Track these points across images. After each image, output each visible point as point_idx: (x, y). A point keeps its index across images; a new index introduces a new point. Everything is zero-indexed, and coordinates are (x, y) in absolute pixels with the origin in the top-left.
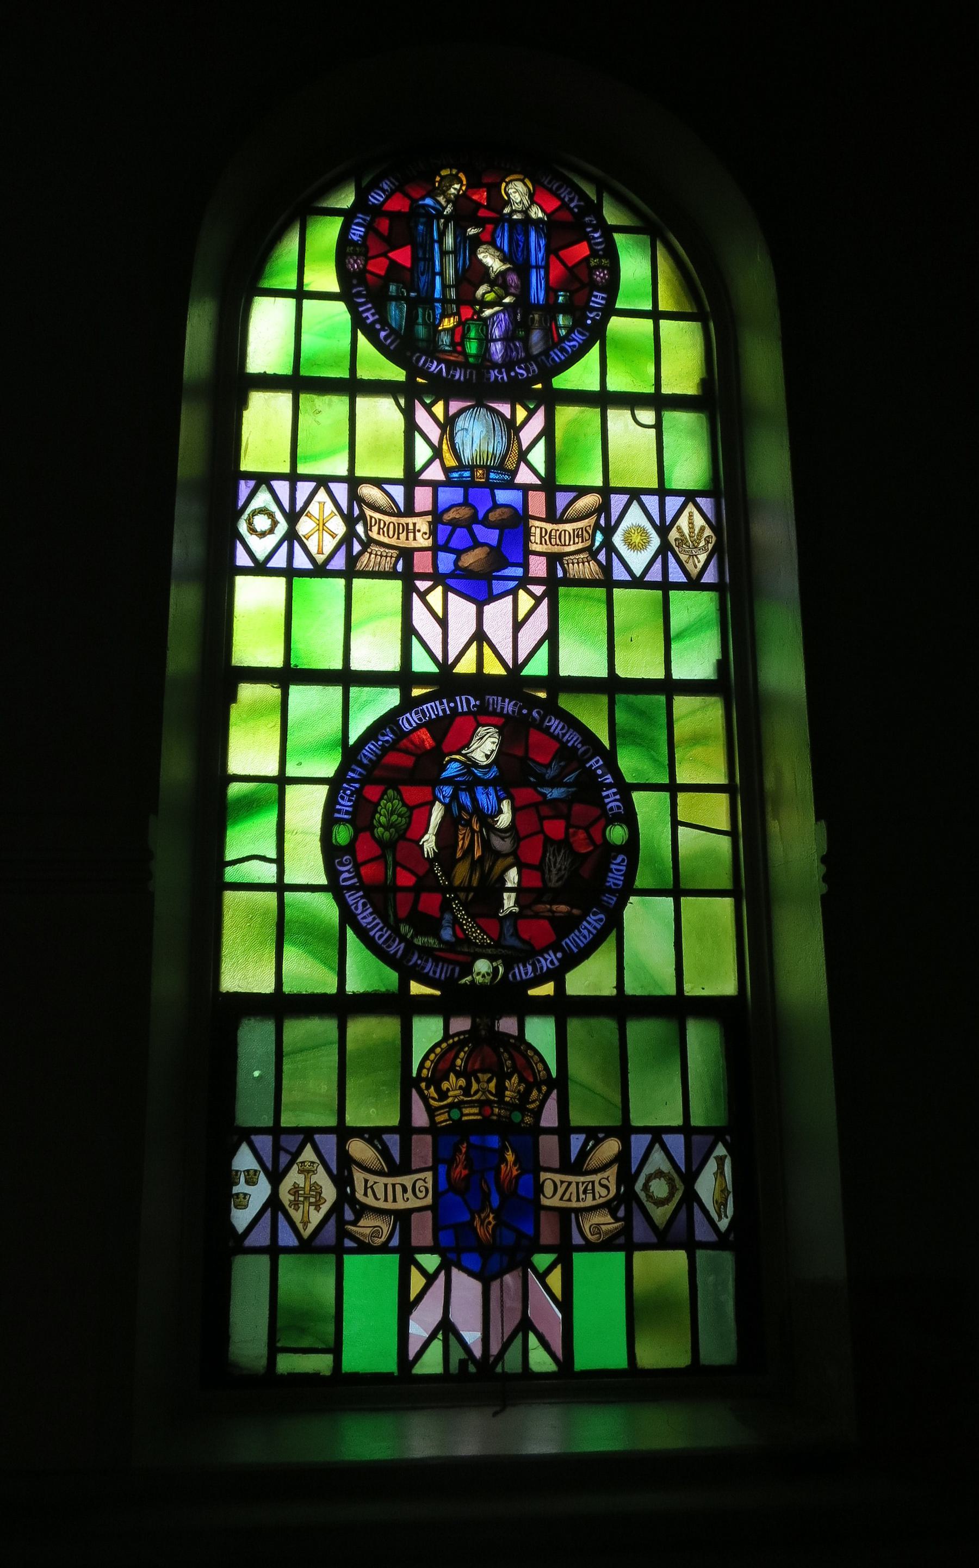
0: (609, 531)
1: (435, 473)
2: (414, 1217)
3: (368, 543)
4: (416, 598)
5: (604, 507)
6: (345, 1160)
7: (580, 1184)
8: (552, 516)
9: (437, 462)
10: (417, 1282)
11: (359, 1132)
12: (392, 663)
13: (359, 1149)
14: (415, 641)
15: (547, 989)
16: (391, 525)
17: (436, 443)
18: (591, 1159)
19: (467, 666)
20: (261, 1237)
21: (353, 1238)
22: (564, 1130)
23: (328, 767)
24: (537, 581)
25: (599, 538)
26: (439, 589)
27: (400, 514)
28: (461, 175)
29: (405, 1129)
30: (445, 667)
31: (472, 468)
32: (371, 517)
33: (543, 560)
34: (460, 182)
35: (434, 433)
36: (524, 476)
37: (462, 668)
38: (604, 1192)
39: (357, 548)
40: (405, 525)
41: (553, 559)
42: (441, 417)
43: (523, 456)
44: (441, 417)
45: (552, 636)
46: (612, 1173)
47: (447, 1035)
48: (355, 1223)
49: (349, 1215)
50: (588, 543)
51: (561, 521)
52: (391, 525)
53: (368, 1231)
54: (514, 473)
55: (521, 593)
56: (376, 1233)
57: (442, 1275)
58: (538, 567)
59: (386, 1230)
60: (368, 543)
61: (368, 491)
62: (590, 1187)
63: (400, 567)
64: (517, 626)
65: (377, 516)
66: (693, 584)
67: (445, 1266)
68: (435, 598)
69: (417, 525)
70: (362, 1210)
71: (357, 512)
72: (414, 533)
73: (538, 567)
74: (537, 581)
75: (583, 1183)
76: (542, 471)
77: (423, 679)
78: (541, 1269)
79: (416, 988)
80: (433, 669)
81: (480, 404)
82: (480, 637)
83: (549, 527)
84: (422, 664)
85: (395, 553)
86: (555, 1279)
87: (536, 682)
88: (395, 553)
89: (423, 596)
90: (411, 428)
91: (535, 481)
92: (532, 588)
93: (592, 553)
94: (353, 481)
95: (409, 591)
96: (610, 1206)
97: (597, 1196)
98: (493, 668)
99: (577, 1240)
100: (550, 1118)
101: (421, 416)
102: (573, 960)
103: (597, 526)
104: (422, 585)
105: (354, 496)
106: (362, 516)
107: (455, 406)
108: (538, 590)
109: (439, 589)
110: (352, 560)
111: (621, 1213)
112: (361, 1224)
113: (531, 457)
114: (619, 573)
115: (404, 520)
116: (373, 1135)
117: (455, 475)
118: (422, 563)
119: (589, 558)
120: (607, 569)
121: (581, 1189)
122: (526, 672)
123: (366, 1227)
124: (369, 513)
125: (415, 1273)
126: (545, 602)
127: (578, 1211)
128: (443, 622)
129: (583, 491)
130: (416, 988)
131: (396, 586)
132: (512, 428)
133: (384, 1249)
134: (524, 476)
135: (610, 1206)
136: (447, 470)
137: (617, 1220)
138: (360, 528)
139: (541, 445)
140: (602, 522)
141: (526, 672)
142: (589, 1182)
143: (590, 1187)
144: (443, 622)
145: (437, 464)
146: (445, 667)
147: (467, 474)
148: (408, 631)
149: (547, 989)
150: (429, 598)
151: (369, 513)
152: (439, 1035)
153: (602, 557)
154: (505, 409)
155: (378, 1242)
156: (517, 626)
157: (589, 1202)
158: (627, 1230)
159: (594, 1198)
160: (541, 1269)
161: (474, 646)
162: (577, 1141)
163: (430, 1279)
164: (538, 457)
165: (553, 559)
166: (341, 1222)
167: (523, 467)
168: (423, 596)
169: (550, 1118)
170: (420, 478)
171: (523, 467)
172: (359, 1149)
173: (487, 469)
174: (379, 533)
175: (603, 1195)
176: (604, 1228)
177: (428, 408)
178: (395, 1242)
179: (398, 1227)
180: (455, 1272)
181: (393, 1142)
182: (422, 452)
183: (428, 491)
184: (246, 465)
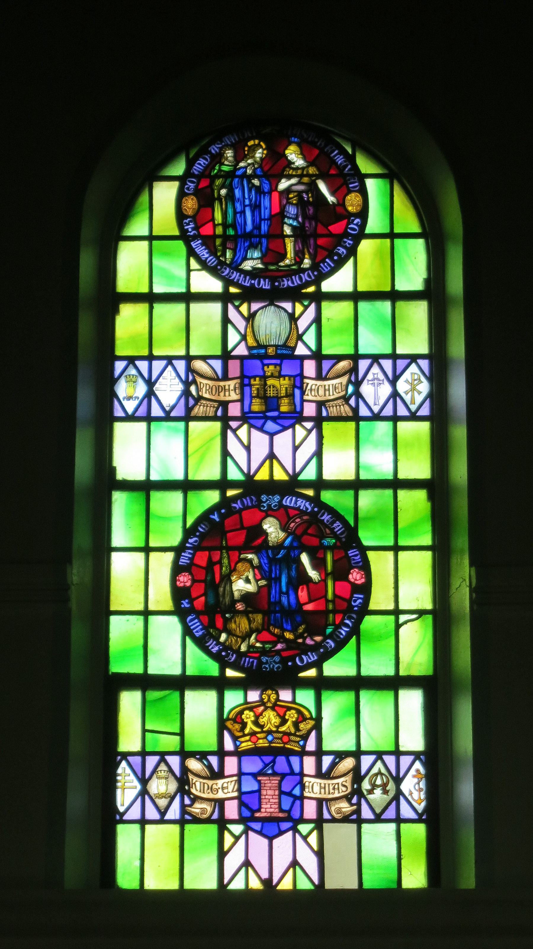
0: (358, 384)
1: (242, 350)
2: (226, 803)
3: (199, 399)
4: (230, 433)
5: (354, 370)
6: (185, 770)
7: (331, 785)
8: (320, 376)
9: (243, 343)
10: (228, 840)
11: (193, 754)
12: (215, 475)
13: (194, 764)
14: (229, 459)
15: (312, 673)
16: (214, 387)
17: (243, 332)
18: (336, 770)
19: (263, 475)
20: (135, 813)
21: (190, 814)
22: (319, 753)
23: (176, 539)
24: (308, 419)
25: (351, 389)
26: (245, 427)
27: (218, 379)
28: (262, 143)
29: (221, 753)
30: (249, 477)
31: (265, 347)
32: (201, 383)
33: (314, 405)
34: (261, 147)
35: (241, 324)
36: (301, 350)
37: (259, 477)
38: (344, 789)
39: (191, 402)
40: (223, 387)
41: (320, 404)
42: (246, 314)
43: (300, 337)
44: (246, 314)
45: (319, 454)
46: (348, 780)
47: (246, 702)
48: (191, 806)
49: (187, 801)
50: (344, 393)
51: (326, 379)
52: (214, 387)
53: (198, 811)
54: (294, 348)
55: (297, 427)
56: (203, 810)
57: (244, 836)
58: (310, 410)
59: (209, 809)
60: (199, 399)
61: (199, 365)
62: (336, 787)
63: (219, 413)
64: (296, 448)
65: (205, 381)
66: (413, 417)
67: (245, 832)
68: (243, 432)
69: (230, 386)
70: (195, 799)
71: (191, 378)
72: (229, 391)
73: (310, 410)
74: (308, 419)
75: (333, 784)
76: (314, 347)
77: (234, 484)
78: (304, 833)
79: (230, 673)
80: (241, 477)
81: (271, 304)
82: (271, 456)
83: (319, 383)
84: (234, 474)
85: (216, 405)
86: (313, 839)
87: (307, 484)
88: (216, 405)
89: (234, 431)
90: (226, 321)
91: (307, 352)
92: (305, 424)
93: (346, 399)
94: (188, 358)
95: (225, 428)
96: (348, 798)
97: (340, 791)
98: (280, 475)
99: (326, 816)
100: (311, 746)
101: (232, 313)
102: (329, 654)
103: (349, 382)
104: (234, 424)
105: (189, 369)
106: (194, 382)
107: (255, 306)
108: (309, 425)
109: (245, 427)
110: (189, 409)
111: (354, 800)
112: (194, 806)
113: (305, 338)
114: (364, 411)
115: (222, 384)
116: (202, 756)
117: (255, 351)
118: (234, 410)
119: (344, 403)
120: (356, 410)
121: (331, 787)
122: (301, 478)
123: (197, 808)
124: (199, 380)
125: (226, 834)
126: (314, 433)
127: (328, 800)
128: (248, 448)
129: (339, 358)
130: (230, 673)
131: (217, 426)
132: (293, 318)
133: (208, 821)
134: (301, 350)
135: (348, 798)
136: (249, 348)
137: (352, 805)
138: (193, 389)
139: (313, 329)
140: (353, 379)
141: (301, 478)
142: (336, 784)
143: (336, 787)
144: (248, 448)
145: (243, 344)
146: (249, 477)
147: (263, 351)
148: (225, 454)
149: (312, 673)
150: (238, 432)
151: (199, 380)
152: (242, 701)
153: (352, 402)
154: (288, 306)
155: (205, 816)
156: (296, 448)
157: (337, 795)
158: (358, 811)
159: (339, 793)
160: (304, 833)
161: (268, 462)
162: (327, 761)
163: (237, 838)
164: (310, 338)
165: (320, 404)
166: (183, 806)
167: (300, 344)
168: (234, 431)
169: (311, 746)
170: (231, 354)
171: (300, 344)
172: (194, 764)
173: (277, 346)
174: (206, 393)
175: (343, 792)
176: (344, 810)
177: (237, 308)
178: (215, 816)
179: (217, 806)
180: (251, 834)
181: (214, 760)
182: (233, 338)
183: (237, 362)
184: (119, 352)
